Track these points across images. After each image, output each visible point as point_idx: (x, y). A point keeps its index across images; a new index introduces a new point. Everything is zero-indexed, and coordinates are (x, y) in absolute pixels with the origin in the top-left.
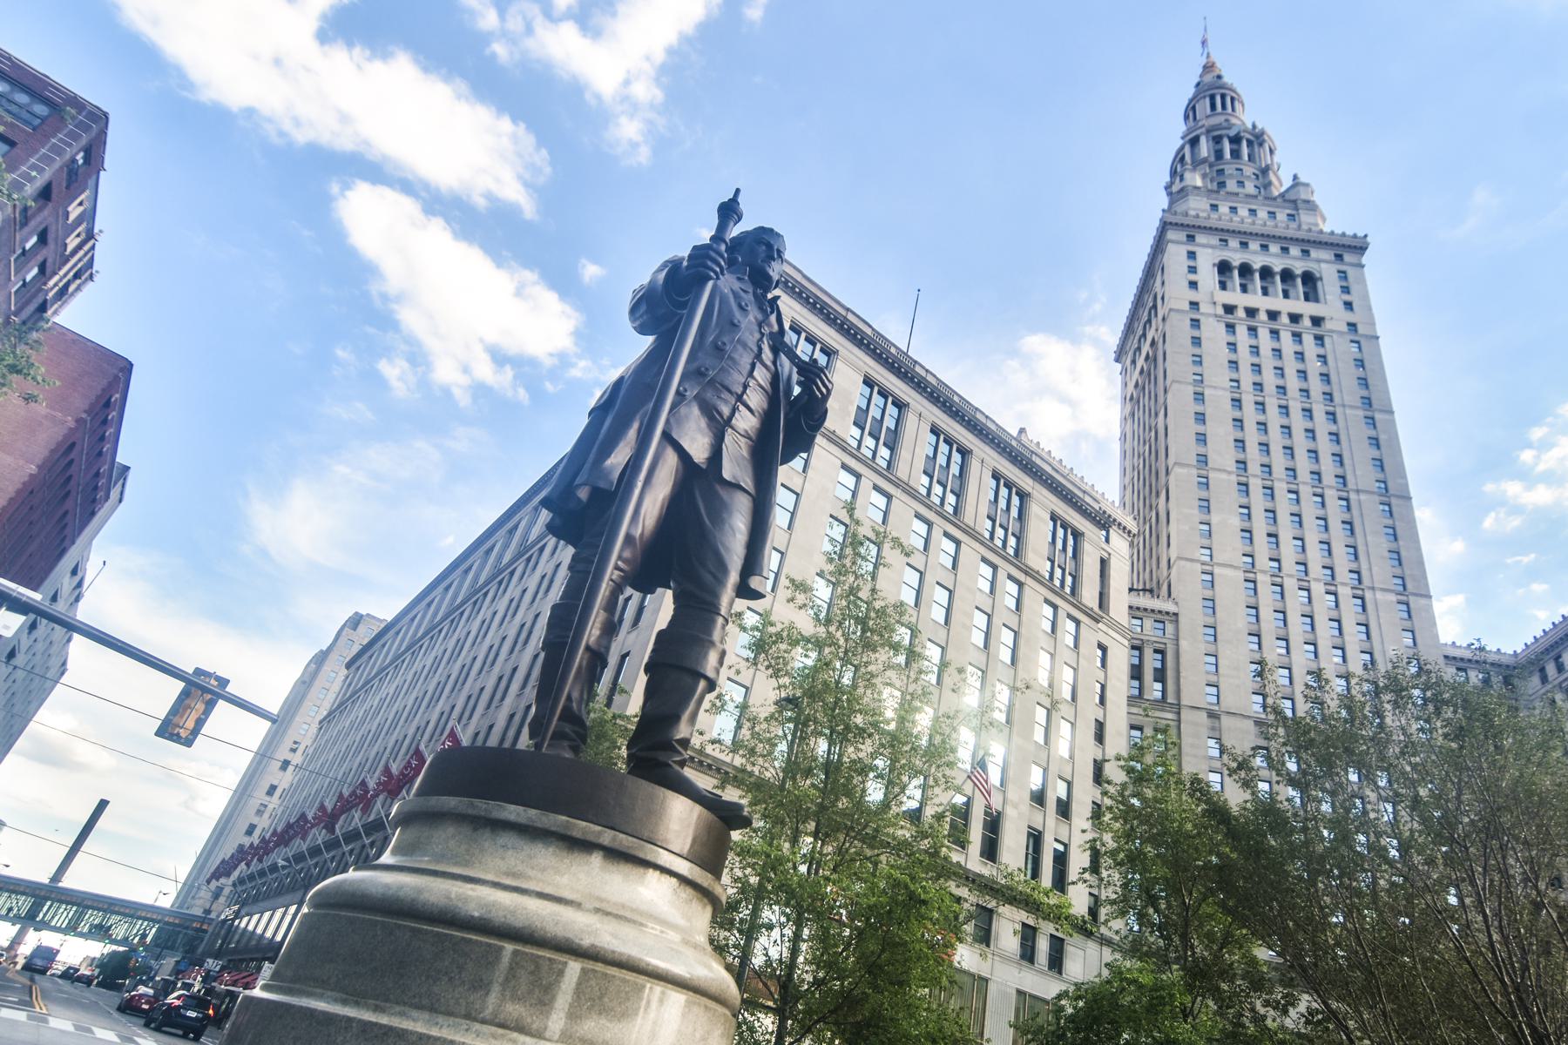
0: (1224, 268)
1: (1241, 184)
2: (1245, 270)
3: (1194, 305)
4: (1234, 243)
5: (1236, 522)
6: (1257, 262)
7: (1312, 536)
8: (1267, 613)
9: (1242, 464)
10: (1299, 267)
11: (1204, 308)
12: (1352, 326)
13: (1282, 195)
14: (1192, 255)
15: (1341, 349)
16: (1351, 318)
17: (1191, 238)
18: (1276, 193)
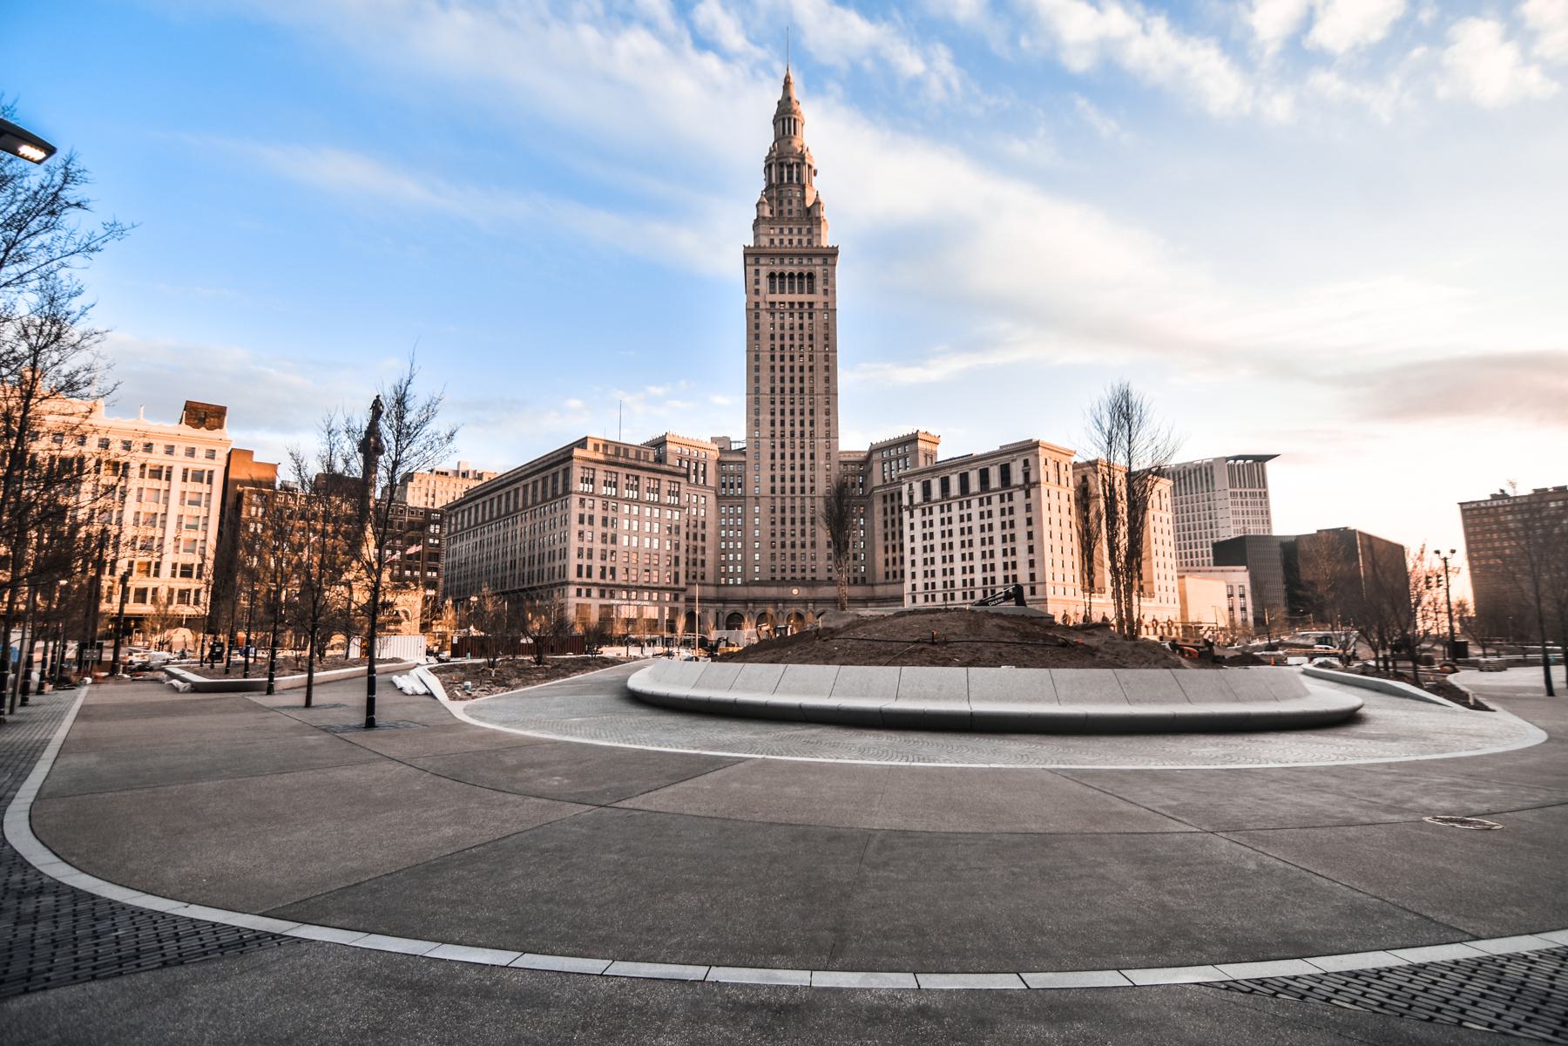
0: (772, 276)
1: (790, 203)
2: (782, 275)
3: (757, 304)
4: (777, 261)
5: (769, 417)
6: (787, 270)
7: (798, 419)
8: (778, 456)
9: (773, 390)
10: (806, 270)
11: (762, 306)
12: (826, 304)
13: (809, 210)
14: (757, 272)
15: (820, 318)
16: (825, 299)
17: (757, 262)
18: (809, 203)
